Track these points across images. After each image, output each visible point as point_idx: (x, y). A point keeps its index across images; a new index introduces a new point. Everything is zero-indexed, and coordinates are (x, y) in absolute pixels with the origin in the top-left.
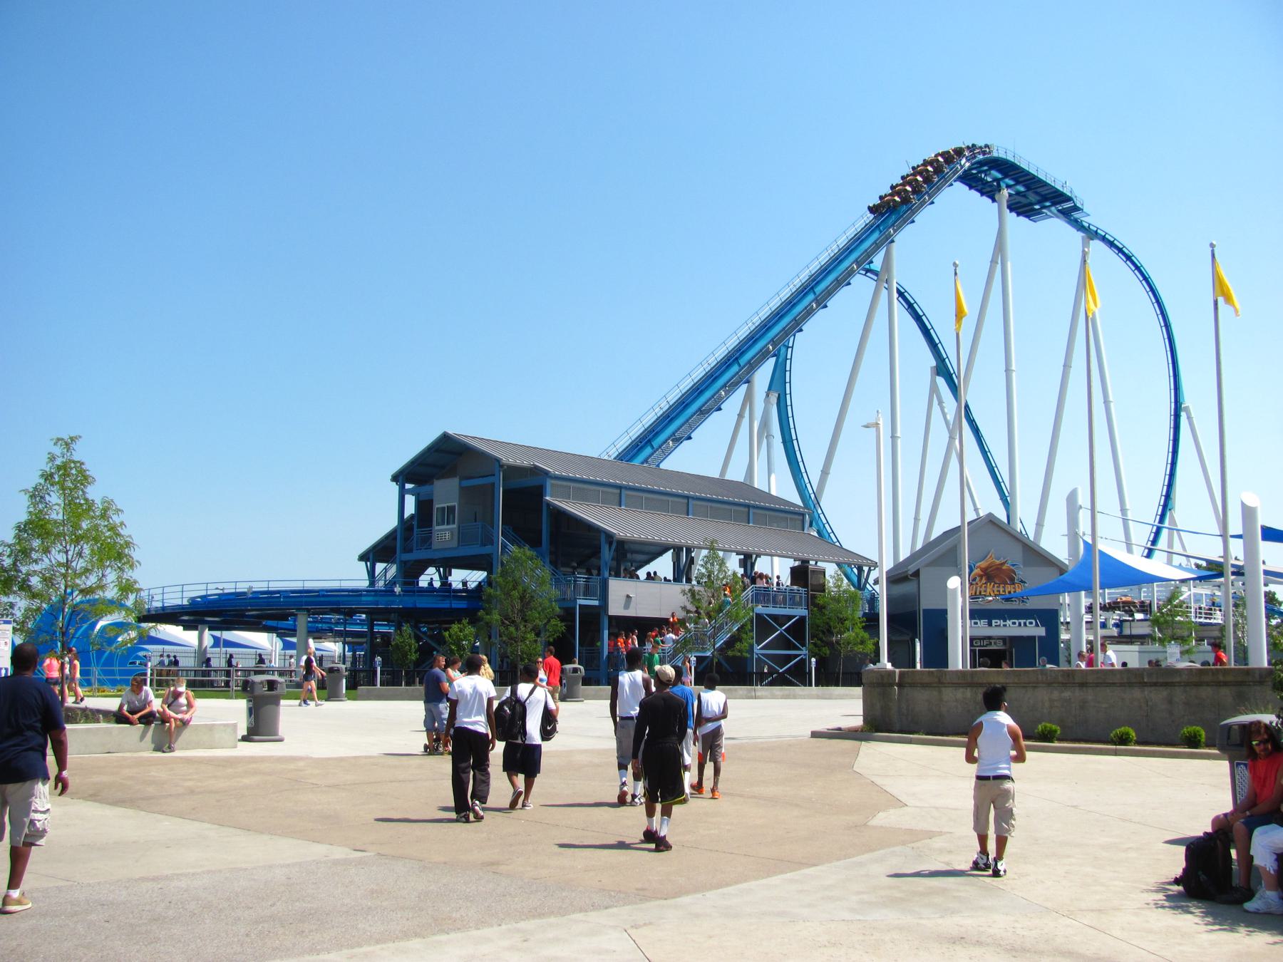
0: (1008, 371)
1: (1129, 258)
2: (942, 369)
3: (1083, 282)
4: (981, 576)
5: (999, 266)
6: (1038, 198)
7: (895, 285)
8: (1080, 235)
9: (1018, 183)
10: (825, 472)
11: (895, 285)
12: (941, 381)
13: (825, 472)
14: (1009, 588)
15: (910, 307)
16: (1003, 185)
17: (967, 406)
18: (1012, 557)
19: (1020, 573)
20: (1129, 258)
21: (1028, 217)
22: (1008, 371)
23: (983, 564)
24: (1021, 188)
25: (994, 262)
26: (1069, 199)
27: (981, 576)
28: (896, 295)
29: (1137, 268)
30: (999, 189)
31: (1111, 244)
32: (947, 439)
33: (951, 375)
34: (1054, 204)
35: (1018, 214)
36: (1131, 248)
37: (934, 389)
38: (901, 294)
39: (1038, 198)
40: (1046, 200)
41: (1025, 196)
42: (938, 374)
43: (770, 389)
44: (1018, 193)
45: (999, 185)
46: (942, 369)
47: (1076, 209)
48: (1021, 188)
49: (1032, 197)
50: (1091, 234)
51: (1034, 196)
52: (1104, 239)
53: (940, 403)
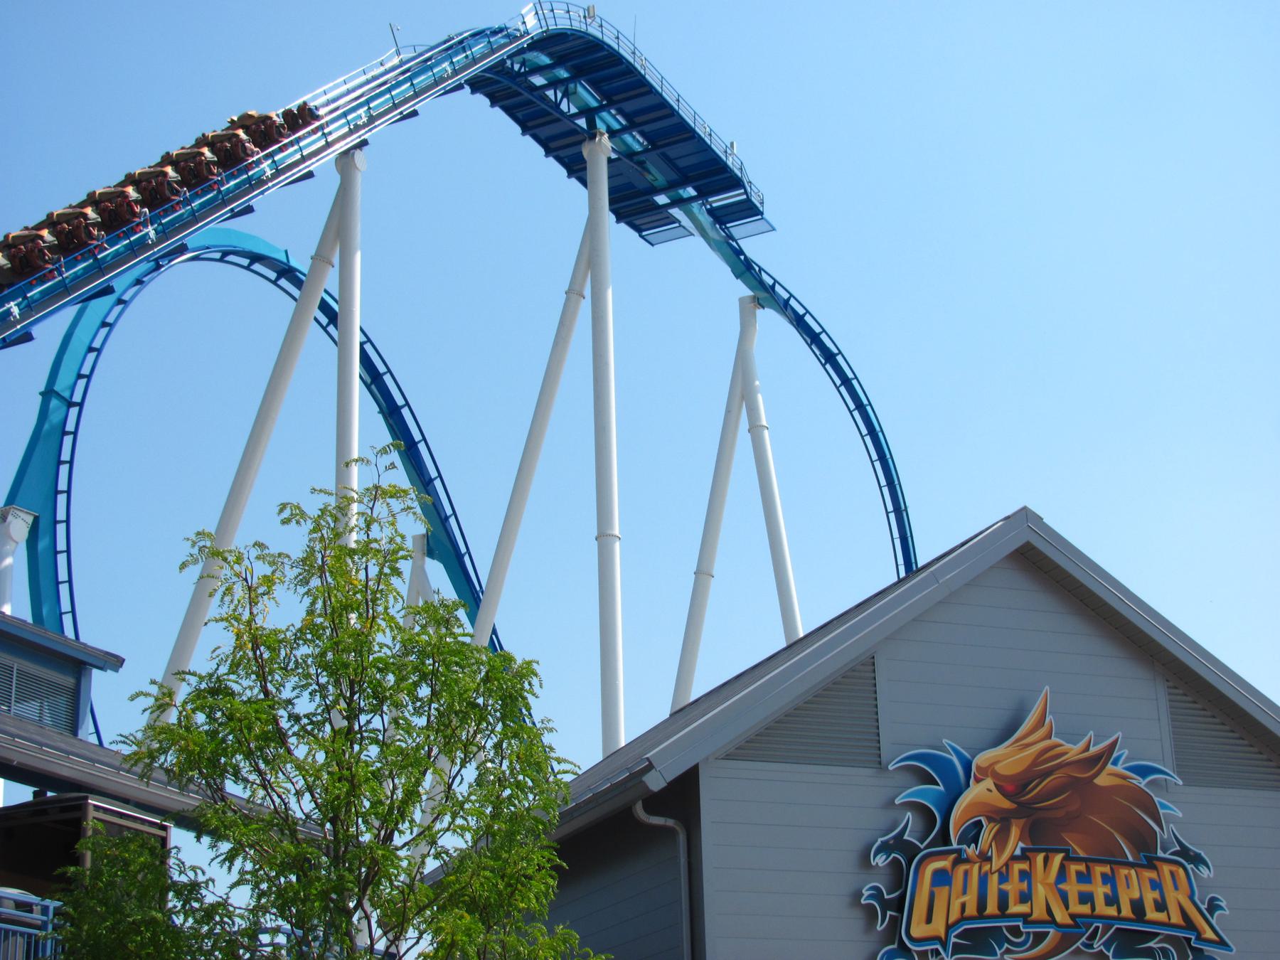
0: (604, 537)
1: (829, 358)
3: (742, 390)
4: (1003, 820)
5: (585, 307)
6: (674, 176)
8: (742, 290)
9: (631, 126)
14: (1134, 886)
16: (601, 126)
17: (494, 632)
18: (1129, 729)
19: (1178, 813)
20: (829, 358)
21: (638, 229)
22: (604, 537)
23: (1009, 758)
24: (635, 141)
25: (573, 293)
26: (735, 182)
27: (1003, 820)
29: (846, 382)
30: (592, 133)
31: (799, 322)
33: (460, 557)
34: (703, 194)
35: (619, 219)
36: (839, 335)
39: (674, 176)
40: (684, 183)
41: (641, 164)
42: (430, 553)
43: (11, 499)
44: (631, 154)
45: (591, 124)
47: (749, 210)
48: (635, 141)
49: (657, 176)
50: (764, 292)
51: (661, 166)
52: (784, 307)
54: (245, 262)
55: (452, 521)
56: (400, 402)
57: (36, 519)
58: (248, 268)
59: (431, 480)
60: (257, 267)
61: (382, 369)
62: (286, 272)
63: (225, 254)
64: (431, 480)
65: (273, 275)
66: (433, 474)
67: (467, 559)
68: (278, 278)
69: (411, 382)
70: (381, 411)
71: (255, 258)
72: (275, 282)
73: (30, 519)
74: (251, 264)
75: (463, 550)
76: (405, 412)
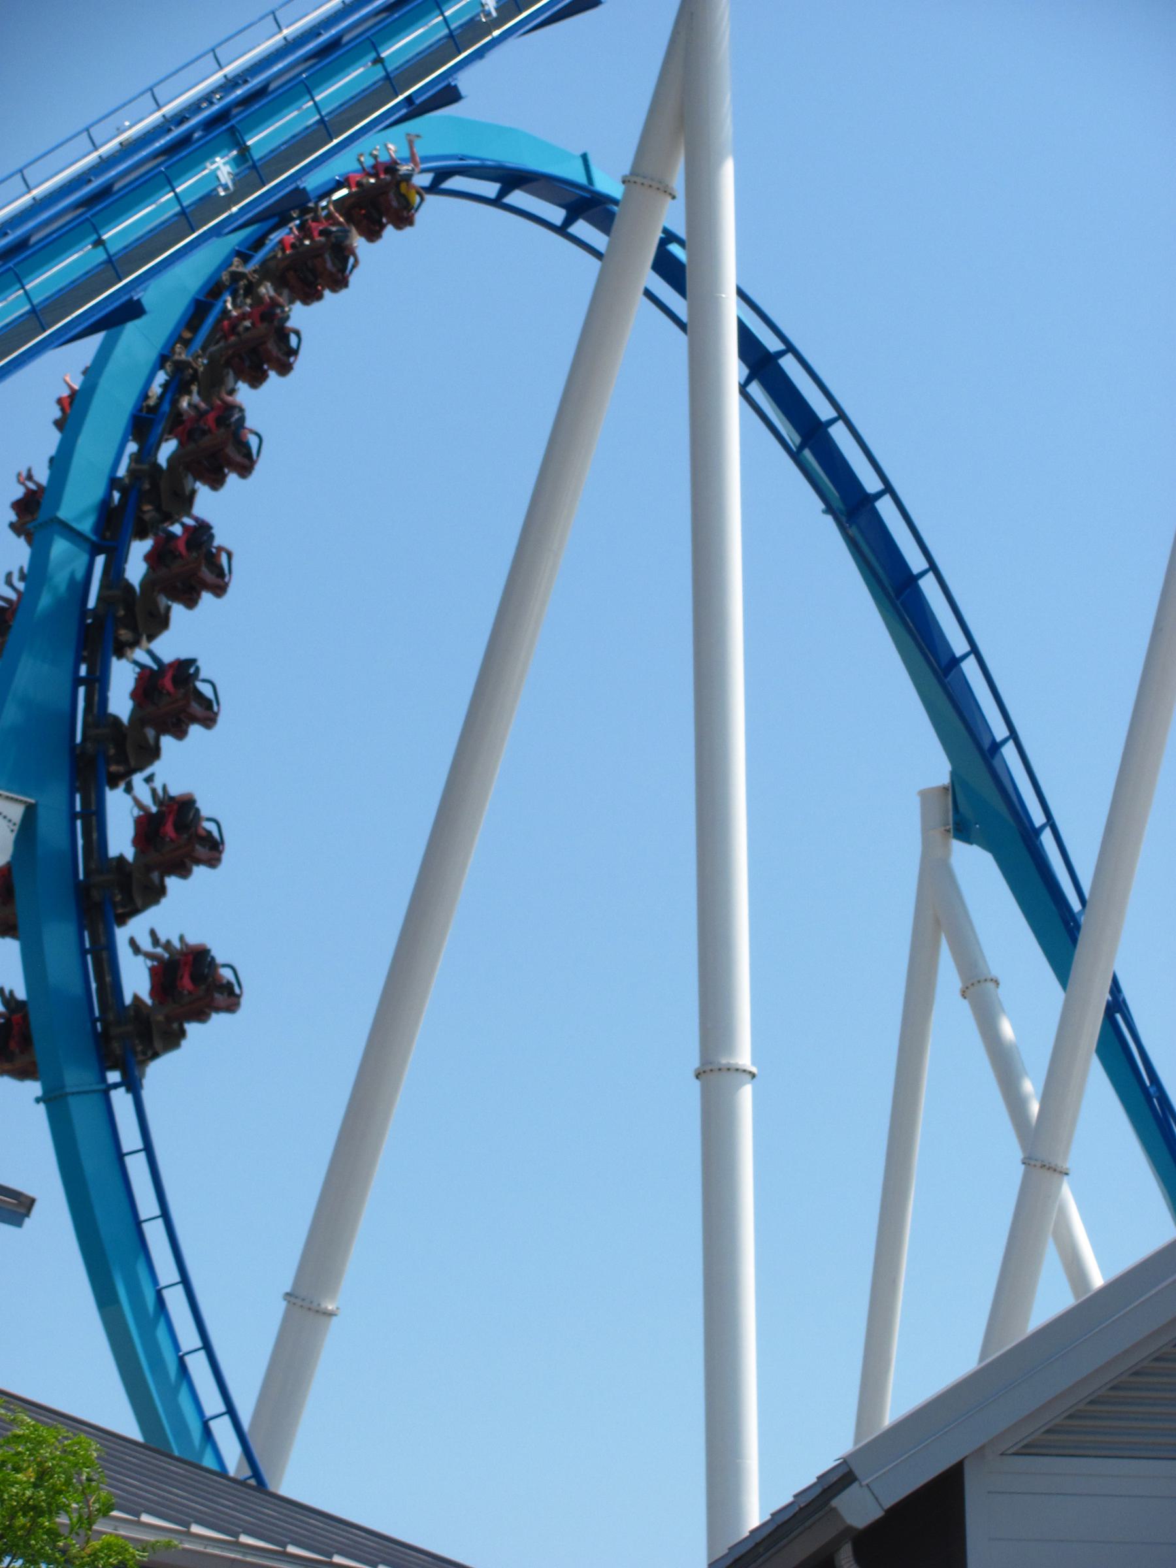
2: (987, 804)
7: (731, 311)
10: (305, 1308)
11: (731, 311)
12: (976, 869)
13: (305, 1308)
15: (810, 439)
17: (1117, 1005)
28: (733, 369)
32: (1017, 1171)
33: (1030, 835)
37: (939, 915)
38: (760, 363)
42: (962, 830)
46: (987, 804)
53: (978, 988)
54: (491, 189)
55: (1009, 752)
56: (872, 484)
57: (30, 812)
58: (496, 202)
59: (955, 662)
60: (517, 198)
61: (824, 412)
62: (586, 204)
63: (442, 175)
64: (955, 662)
65: (557, 215)
66: (959, 645)
67: (1047, 838)
68: (569, 221)
69: (890, 437)
70: (829, 509)
71: (513, 179)
72: (561, 230)
73: (16, 812)
74: (503, 193)
75: (1038, 818)
76: (885, 506)
